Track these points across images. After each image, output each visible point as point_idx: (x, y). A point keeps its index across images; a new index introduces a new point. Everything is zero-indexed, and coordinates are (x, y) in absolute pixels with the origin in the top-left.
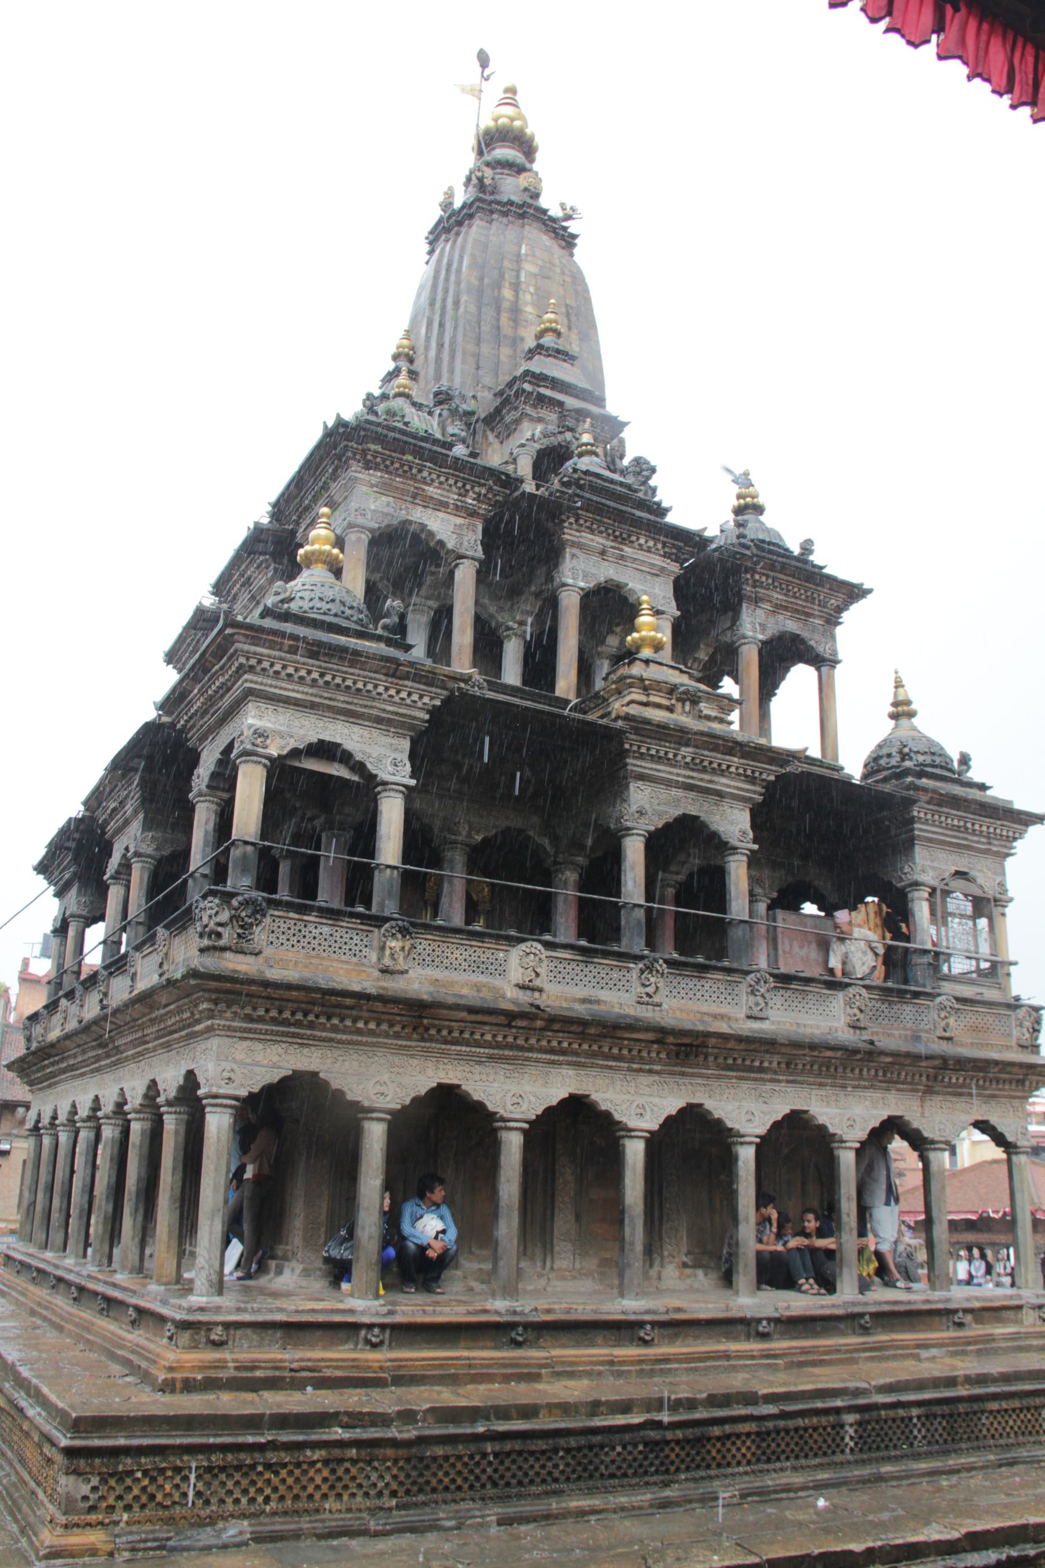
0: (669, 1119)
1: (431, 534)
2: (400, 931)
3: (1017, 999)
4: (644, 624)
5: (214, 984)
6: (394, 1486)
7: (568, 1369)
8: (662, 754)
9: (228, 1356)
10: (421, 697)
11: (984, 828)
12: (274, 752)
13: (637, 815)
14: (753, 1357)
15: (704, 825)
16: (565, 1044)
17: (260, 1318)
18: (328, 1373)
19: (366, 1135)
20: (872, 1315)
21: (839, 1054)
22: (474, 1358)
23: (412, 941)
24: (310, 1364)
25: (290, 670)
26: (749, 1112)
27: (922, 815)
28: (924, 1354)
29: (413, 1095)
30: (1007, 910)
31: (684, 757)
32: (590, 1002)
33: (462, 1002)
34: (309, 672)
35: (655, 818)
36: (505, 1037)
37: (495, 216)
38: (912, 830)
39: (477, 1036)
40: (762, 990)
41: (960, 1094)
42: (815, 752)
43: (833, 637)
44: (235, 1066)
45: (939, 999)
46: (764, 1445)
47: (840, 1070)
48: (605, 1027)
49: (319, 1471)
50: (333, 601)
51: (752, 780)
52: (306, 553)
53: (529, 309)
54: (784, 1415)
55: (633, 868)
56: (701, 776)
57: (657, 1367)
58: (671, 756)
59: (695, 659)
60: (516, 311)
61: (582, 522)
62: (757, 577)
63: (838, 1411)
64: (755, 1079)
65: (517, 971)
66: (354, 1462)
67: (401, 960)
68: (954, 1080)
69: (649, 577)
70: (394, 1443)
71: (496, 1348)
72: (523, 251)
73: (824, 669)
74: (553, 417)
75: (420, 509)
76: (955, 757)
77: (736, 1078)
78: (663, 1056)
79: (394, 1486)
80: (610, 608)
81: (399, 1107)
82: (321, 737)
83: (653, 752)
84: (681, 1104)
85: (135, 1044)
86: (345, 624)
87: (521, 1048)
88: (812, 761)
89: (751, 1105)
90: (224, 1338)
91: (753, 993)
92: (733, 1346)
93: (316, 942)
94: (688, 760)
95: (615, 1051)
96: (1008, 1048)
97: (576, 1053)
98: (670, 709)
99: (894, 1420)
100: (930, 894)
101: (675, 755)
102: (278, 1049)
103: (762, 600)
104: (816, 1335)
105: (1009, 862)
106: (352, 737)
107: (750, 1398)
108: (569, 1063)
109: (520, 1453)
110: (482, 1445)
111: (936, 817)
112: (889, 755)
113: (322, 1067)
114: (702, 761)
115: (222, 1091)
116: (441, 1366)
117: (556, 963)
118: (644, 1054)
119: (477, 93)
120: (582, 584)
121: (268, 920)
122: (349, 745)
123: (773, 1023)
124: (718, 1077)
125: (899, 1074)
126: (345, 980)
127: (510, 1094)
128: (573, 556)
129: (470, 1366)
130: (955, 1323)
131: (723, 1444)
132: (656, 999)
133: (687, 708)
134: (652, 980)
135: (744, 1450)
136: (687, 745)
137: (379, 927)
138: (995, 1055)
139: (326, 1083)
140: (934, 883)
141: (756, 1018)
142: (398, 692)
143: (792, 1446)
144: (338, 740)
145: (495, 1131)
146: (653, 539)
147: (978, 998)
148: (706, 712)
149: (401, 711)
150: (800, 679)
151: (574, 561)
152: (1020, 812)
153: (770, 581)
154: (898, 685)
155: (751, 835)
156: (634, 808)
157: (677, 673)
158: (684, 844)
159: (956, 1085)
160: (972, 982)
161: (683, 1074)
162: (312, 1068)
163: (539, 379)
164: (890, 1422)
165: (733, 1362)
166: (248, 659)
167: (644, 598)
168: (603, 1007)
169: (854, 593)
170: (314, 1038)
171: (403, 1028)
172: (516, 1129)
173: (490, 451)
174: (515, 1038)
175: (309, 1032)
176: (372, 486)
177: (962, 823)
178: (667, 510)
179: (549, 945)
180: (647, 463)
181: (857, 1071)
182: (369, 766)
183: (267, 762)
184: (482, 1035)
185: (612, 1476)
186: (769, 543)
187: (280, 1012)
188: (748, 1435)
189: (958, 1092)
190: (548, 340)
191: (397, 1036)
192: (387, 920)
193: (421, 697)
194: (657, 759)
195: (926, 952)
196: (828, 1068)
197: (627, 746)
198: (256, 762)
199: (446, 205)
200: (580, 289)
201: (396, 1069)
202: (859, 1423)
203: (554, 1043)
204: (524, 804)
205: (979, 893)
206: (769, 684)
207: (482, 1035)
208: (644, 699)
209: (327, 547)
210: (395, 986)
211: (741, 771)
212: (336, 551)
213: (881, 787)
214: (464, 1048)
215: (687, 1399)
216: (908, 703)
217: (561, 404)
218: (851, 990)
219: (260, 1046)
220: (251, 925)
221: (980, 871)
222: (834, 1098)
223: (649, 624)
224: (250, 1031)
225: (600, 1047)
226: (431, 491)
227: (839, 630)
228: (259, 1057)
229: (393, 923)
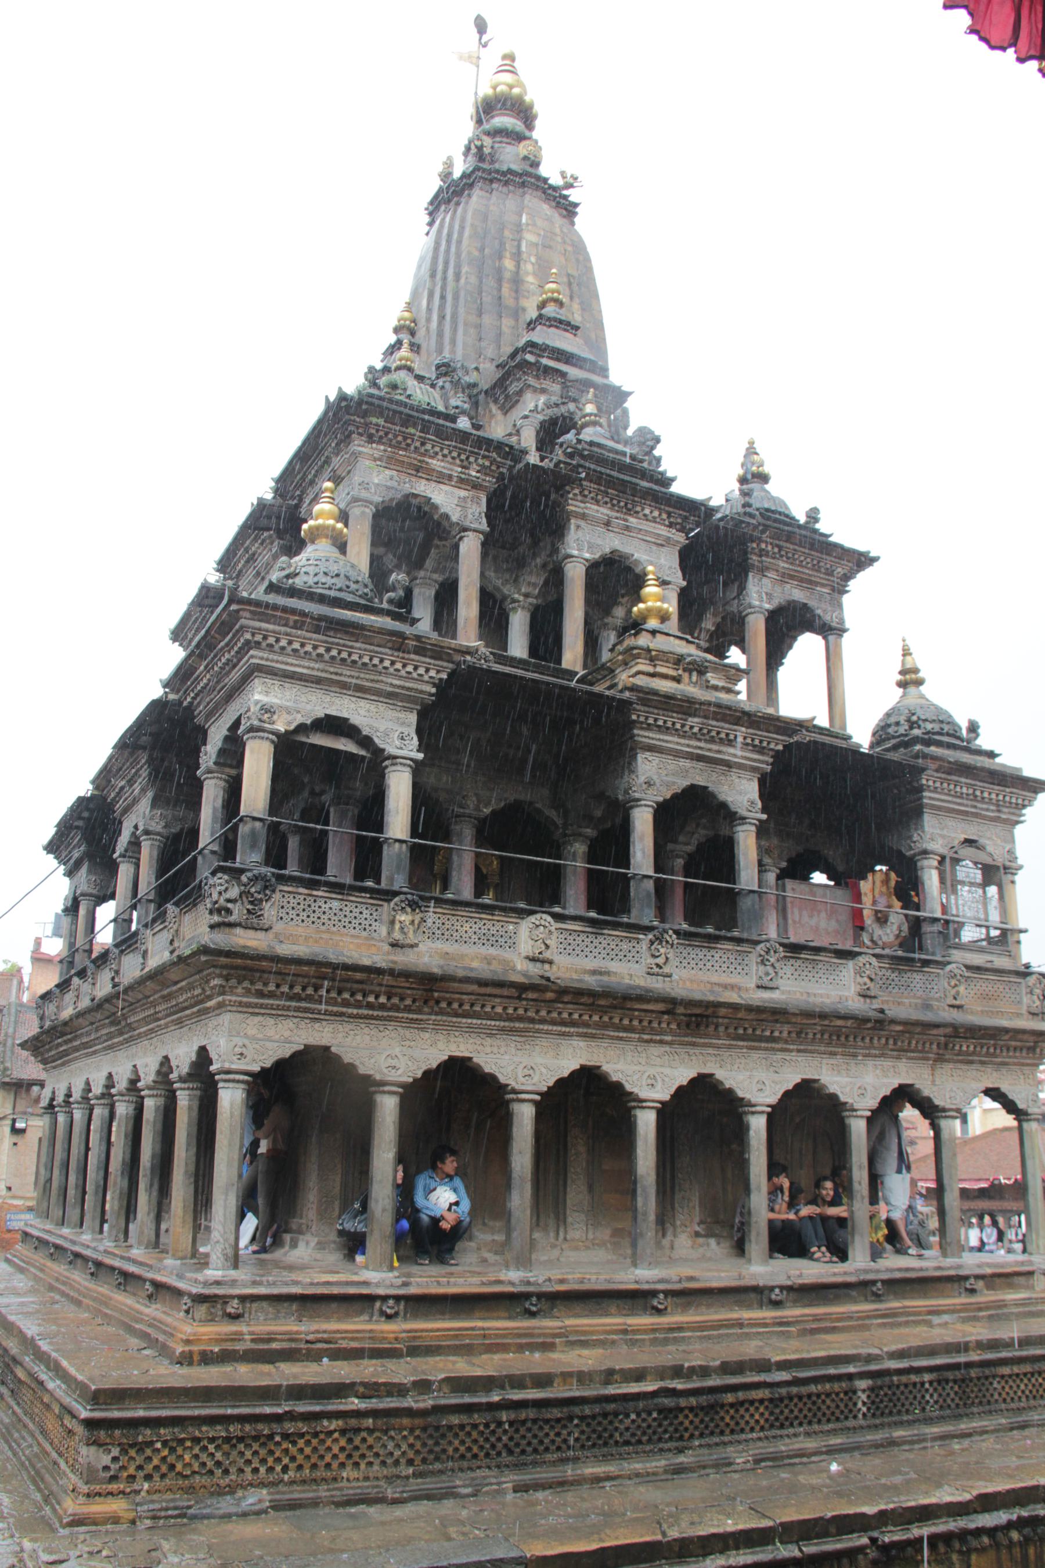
0: (680, 1089)
1: (435, 507)
2: (410, 906)
3: (1027, 966)
5: (223, 960)
6: (411, 1454)
8: (669, 724)
9: (244, 1329)
10: (427, 670)
11: (993, 796)
12: (281, 727)
13: (645, 786)
14: (765, 1325)
15: (713, 795)
16: (576, 1016)
17: (275, 1291)
18: (344, 1344)
19: (378, 1108)
20: (884, 1282)
21: (849, 1023)
22: (489, 1329)
23: (421, 915)
24: (325, 1336)
27: (931, 783)
28: (936, 1320)
29: (424, 1068)
30: (1017, 878)
31: (692, 727)
32: (601, 973)
33: (472, 975)
34: (315, 647)
35: (663, 789)
36: (516, 1009)
37: (495, 186)
38: (921, 798)
39: (488, 1009)
40: (772, 960)
41: (971, 1062)
42: (823, 721)
43: (840, 606)
44: (246, 1042)
45: (949, 968)
46: (777, 1411)
47: (851, 1038)
48: (615, 998)
49: (336, 1440)
50: (337, 575)
51: (761, 750)
52: (310, 528)
53: (530, 279)
54: (797, 1382)
55: (642, 839)
58: (678, 726)
60: (517, 281)
62: (763, 546)
63: (850, 1377)
64: (766, 1049)
66: (370, 1431)
67: (411, 934)
68: (964, 1048)
69: (654, 548)
70: (409, 1412)
71: (510, 1318)
72: (524, 221)
73: (831, 638)
74: (556, 388)
75: (424, 482)
76: (964, 725)
77: (747, 1048)
78: (674, 1026)
79: (411, 1454)
80: (615, 580)
81: (411, 1080)
82: (328, 712)
83: (660, 723)
84: (692, 1074)
85: (146, 1021)
86: (350, 598)
87: (532, 1021)
88: (821, 730)
89: (762, 1074)
90: (241, 1311)
91: (762, 962)
92: (746, 1315)
93: (326, 917)
94: (696, 730)
95: (626, 1022)
96: (1018, 1015)
98: (677, 680)
99: (906, 1386)
100: (941, 863)
101: (683, 726)
102: (290, 1023)
103: (767, 568)
104: (827, 1301)
105: (1018, 830)
107: (763, 1366)
109: (535, 1421)
110: (497, 1414)
111: (945, 785)
112: (897, 724)
113: (334, 1042)
114: (709, 731)
115: (234, 1067)
116: (456, 1336)
117: (566, 934)
118: (655, 1025)
119: (476, 61)
120: (587, 556)
121: (277, 896)
122: (356, 720)
123: (783, 993)
124: (730, 1047)
125: (909, 1043)
126: (355, 955)
127: (521, 1066)
128: (578, 527)
129: (484, 1336)
130: (966, 1289)
131: (737, 1411)
132: (666, 970)
133: (694, 678)
134: (662, 950)
135: (757, 1417)
136: (695, 716)
137: (389, 901)
138: (1005, 1023)
139: (338, 1057)
141: (766, 988)
142: (404, 666)
143: (805, 1412)
144: (345, 715)
147: (989, 965)
148: (713, 682)
149: (407, 685)
150: (807, 647)
151: (580, 533)
154: (906, 653)
155: (759, 805)
156: (642, 779)
157: (684, 643)
158: (690, 812)
159: (968, 1054)
160: (982, 950)
161: (694, 1045)
162: (324, 1042)
164: (902, 1388)
166: (253, 635)
167: (650, 568)
168: (613, 979)
169: (862, 561)
171: (414, 1001)
173: (493, 424)
176: (375, 460)
177: (971, 791)
178: (673, 480)
179: (558, 917)
180: (652, 433)
181: (867, 1040)
182: (376, 740)
183: (274, 738)
184: (493, 1007)
185: (627, 1443)
188: (761, 1401)
189: (967, 1060)
190: (550, 310)
191: (408, 1009)
192: (396, 894)
193: (427, 670)
194: (664, 729)
195: (936, 920)
196: (838, 1037)
197: (634, 717)
199: (446, 176)
200: (581, 258)
201: (407, 1043)
202: (872, 1389)
203: (565, 1015)
204: (532, 774)
205: (988, 861)
206: (775, 654)
207: (493, 1007)
208: (651, 669)
209: (331, 522)
210: (404, 959)
211: (749, 741)
212: (340, 525)
213: (890, 756)
215: (700, 1366)
216: (916, 671)
217: (563, 375)
218: (862, 959)
219: (272, 1021)
220: (261, 900)
222: (844, 1067)
224: (261, 1006)
225: (611, 1018)
226: (436, 464)
227: (846, 599)
228: (271, 1032)
229: (402, 897)
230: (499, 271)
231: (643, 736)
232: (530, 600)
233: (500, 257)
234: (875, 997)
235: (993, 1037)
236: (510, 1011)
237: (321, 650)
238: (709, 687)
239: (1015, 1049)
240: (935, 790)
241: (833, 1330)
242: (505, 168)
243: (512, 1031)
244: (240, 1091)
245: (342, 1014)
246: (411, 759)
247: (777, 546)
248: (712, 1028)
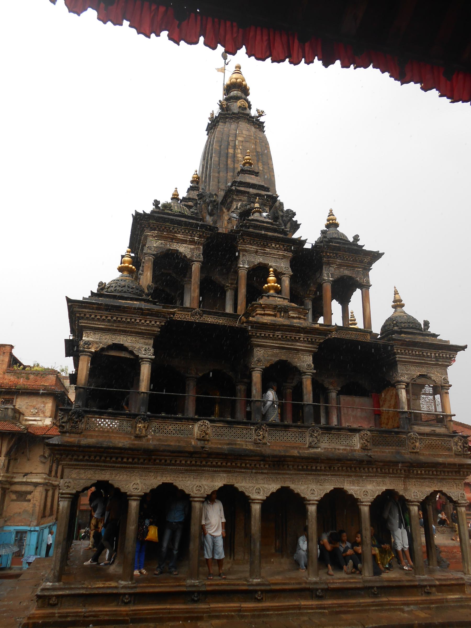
1: (181, 253)
2: (143, 420)
4: (270, 280)
5: (57, 448)
7: (217, 614)
8: (267, 335)
14: (312, 609)
15: (290, 363)
17: (73, 592)
20: (378, 587)
21: (354, 462)
22: (172, 609)
23: (148, 424)
24: (93, 613)
25: (98, 317)
26: (312, 490)
28: (406, 609)
29: (151, 488)
31: (278, 336)
32: (232, 444)
34: (107, 317)
36: (191, 462)
37: (227, 120)
41: (425, 478)
44: (71, 480)
47: (358, 469)
50: (124, 286)
51: (312, 343)
53: (239, 155)
55: (255, 385)
56: (287, 343)
57: (262, 613)
58: (271, 336)
59: (310, 291)
61: (245, 241)
64: (314, 475)
65: (197, 432)
68: (419, 472)
71: (185, 603)
72: (237, 133)
73: (363, 289)
77: (305, 474)
78: (267, 466)
83: (263, 335)
89: (314, 486)
92: (303, 603)
96: (450, 456)
97: (225, 467)
98: (275, 316)
100: (406, 386)
101: (273, 335)
103: (332, 263)
106: (126, 341)
108: (223, 471)
113: (110, 479)
114: (286, 337)
118: (258, 466)
119: (223, 70)
120: (247, 266)
122: (126, 344)
124: (296, 474)
125: (389, 470)
126: (117, 442)
127: (195, 486)
128: (243, 255)
129: (169, 613)
132: (265, 441)
133: (282, 314)
134: (261, 433)
137: (135, 418)
138: (441, 460)
140: (407, 380)
141: (313, 447)
142: (146, 321)
144: (122, 343)
145: (191, 501)
146: (278, 244)
148: (292, 315)
149: (147, 328)
150: (357, 295)
151: (244, 258)
152: (452, 346)
153: (335, 255)
154: (396, 293)
157: (282, 300)
163: (241, 184)
165: (301, 611)
166: (80, 314)
168: (238, 447)
169: (376, 256)
170: (106, 466)
171: (144, 460)
172: (198, 501)
174: (196, 462)
175: (103, 464)
176: (154, 237)
179: (211, 421)
181: (366, 469)
182: (135, 352)
184: (181, 461)
186: (338, 239)
187: (90, 457)
189: (421, 478)
190: (247, 167)
191: (142, 464)
193: (156, 322)
194: (265, 337)
195: (407, 412)
196: (351, 468)
197: (250, 334)
198: (85, 355)
200: (264, 144)
201: (143, 478)
203: (214, 463)
207: (181, 461)
208: (263, 312)
210: (142, 443)
211: (306, 339)
214: (173, 467)
217: (248, 193)
218: (362, 433)
220: (77, 422)
221: (433, 374)
222: (356, 482)
223: (272, 280)
224: (78, 465)
225: (236, 464)
227: (371, 273)
228: (82, 476)
229: (139, 417)
230: (227, 154)
231: (256, 341)
232: (233, 286)
233: (228, 149)
234: (370, 450)
235: (433, 467)
236: (189, 462)
237: (109, 318)
238: (289, 317)
239: (448, 472)
240: (402, 354)
241: (348, 612)
243: (191, 471)
245: (114, 467)
246: (149, 359)
247: (335, 253)
248: (286, 467)
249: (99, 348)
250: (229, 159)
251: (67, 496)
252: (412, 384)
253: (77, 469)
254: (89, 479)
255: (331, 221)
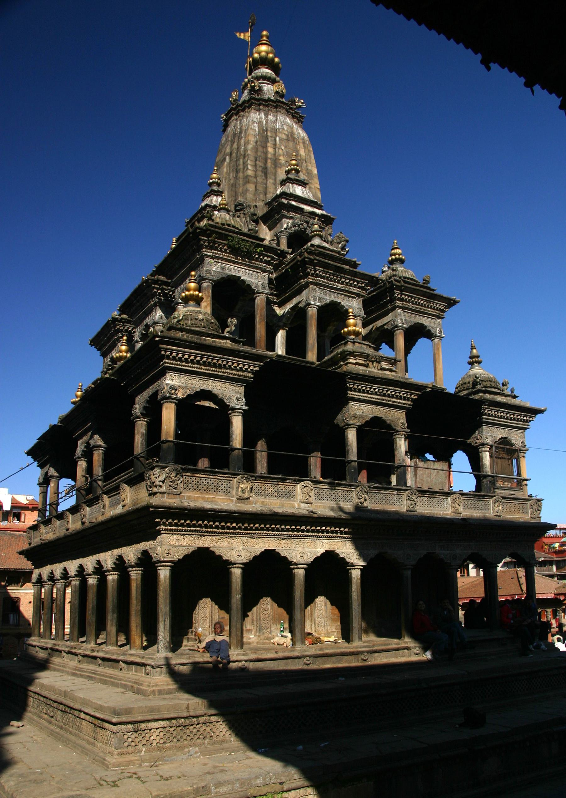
12: (180, 395)
44: (171, 547)
50: (203, 320)
53: (281, 158)
82: (202, 388)
93: (206, 487)
102: (191, 538)
122: (215, 391)
139: (213, 552)
140: (491, 443)
162: (207, 545)
177: (505, 415)
182: (225, 401)
190: (292, 176)
198: (172, 402)
217: (302, 209)
219: (182, 537)
224: (177, 530)
228: (182, 543)
242: (266, 97)
244: (169, 571)
249: (186, 395)
250: (269, 161)
251: (169, 564)
252: (495, 447)
253: (175, 534)
254: (189, 546)
255: (397, 256)
